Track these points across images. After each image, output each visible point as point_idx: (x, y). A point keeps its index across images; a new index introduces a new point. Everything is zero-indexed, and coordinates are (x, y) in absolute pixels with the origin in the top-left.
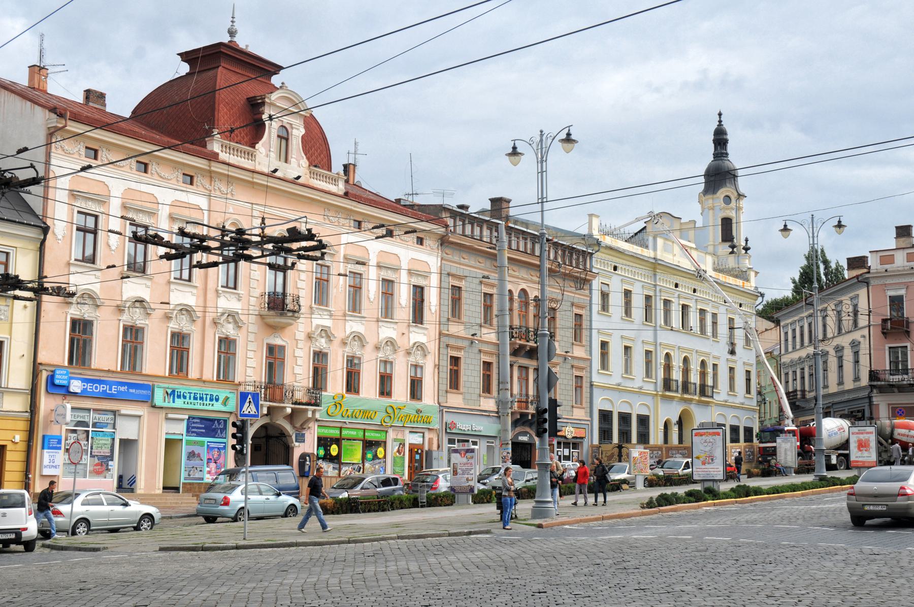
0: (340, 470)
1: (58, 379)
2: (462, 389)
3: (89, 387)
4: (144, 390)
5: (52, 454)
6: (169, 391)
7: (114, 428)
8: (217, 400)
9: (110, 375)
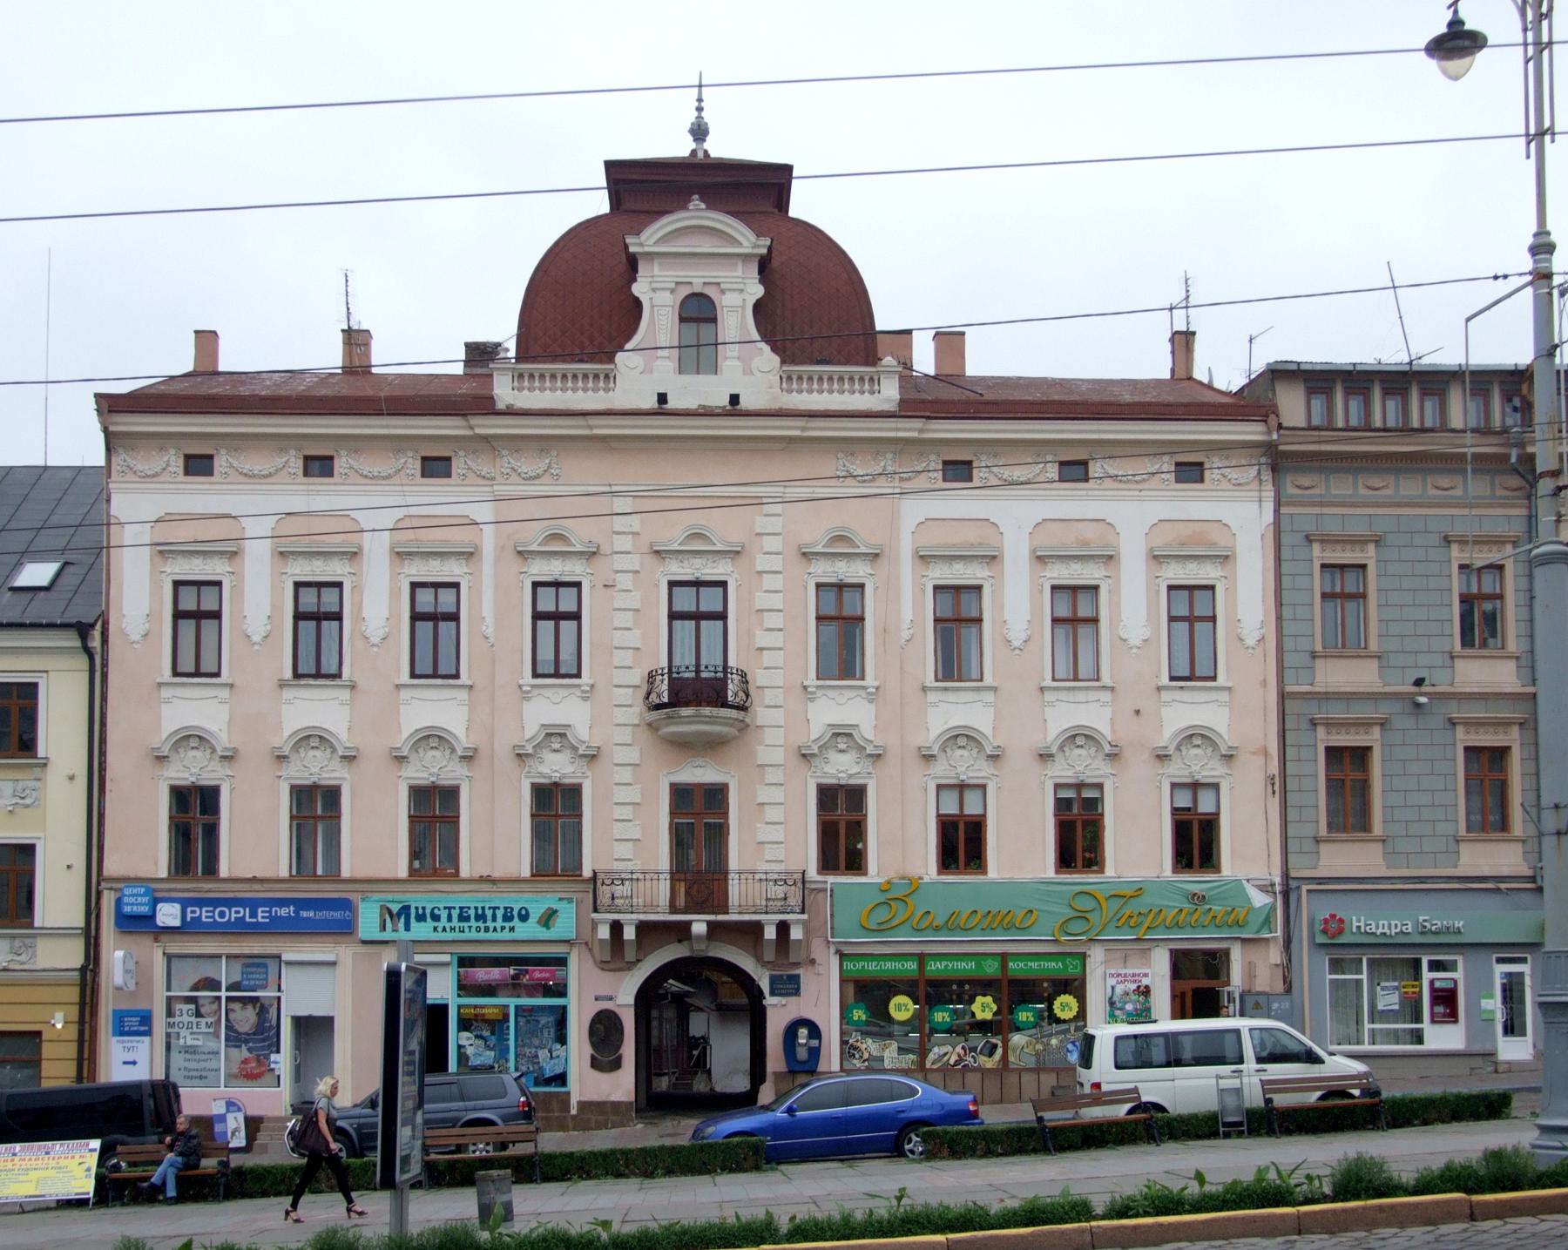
0: (923, 1053)
1: (128, 904)
2: (1378, 828)
3: (204, 914)
4: (336, 910)
5: (129, 1045)
6: (395, 908)
7: (279, 990)
8: (524, 917)
9: (256, 886)
